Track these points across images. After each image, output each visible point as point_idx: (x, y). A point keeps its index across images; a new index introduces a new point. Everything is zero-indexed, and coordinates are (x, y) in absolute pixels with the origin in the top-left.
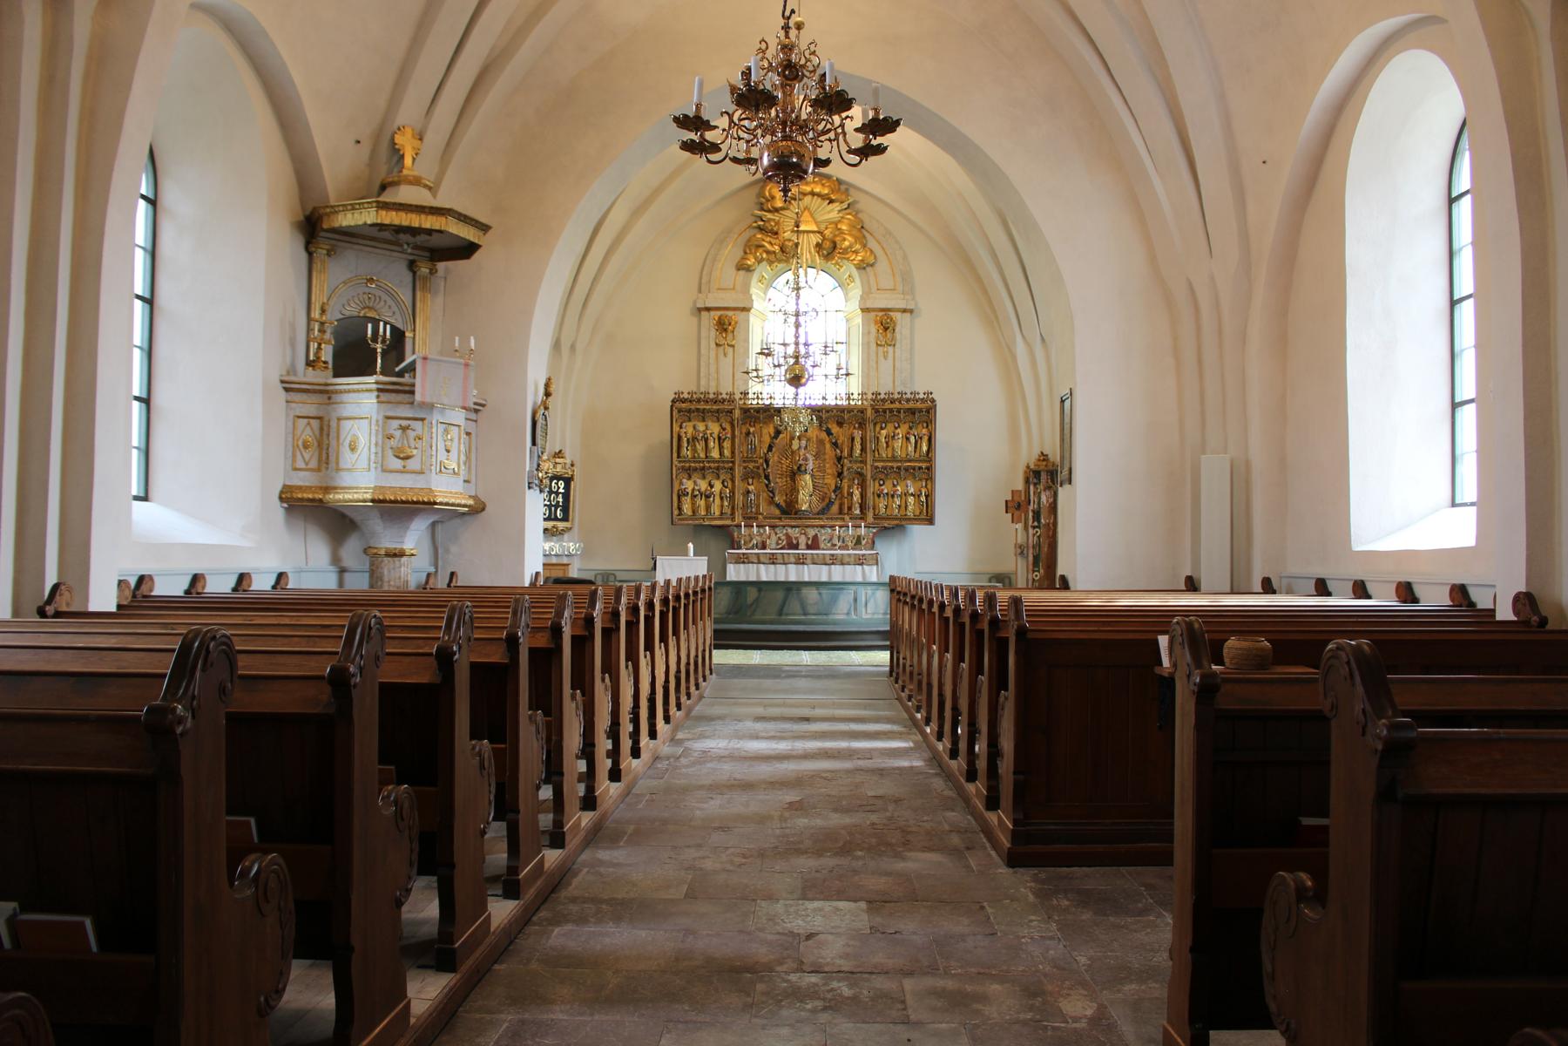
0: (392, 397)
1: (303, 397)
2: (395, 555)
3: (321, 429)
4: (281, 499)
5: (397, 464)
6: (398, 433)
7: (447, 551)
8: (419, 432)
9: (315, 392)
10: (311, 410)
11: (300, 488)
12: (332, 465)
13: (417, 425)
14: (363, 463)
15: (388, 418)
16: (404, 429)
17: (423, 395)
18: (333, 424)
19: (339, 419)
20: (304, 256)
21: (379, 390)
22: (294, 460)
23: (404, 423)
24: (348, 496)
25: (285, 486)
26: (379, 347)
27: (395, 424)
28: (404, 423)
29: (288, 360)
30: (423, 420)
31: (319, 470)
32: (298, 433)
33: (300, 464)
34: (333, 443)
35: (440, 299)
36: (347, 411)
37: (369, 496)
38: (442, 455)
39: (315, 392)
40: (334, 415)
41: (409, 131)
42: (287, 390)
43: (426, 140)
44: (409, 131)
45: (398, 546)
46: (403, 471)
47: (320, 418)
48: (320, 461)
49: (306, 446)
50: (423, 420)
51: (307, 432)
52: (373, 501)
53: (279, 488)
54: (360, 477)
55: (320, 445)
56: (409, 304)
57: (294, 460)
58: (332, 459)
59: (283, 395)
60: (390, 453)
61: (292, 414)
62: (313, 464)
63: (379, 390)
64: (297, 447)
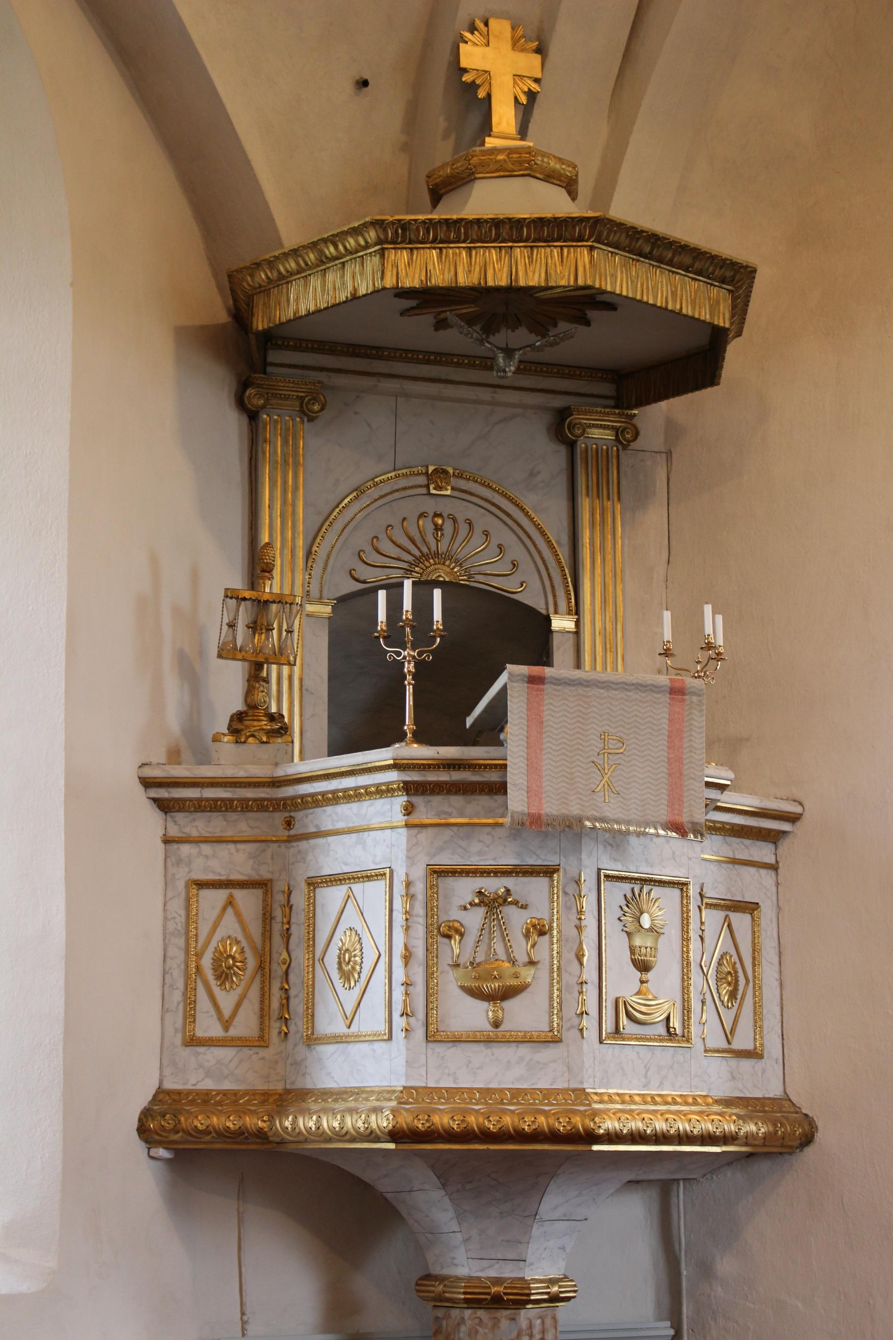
0: (455, 809)
1: (216, 824)
2: (497, 1302)
3: (267, 917)
4: (142, 1130)
5: (474, 1015)
6: (474, 919)
7: (706, 1270)
8: (540, 910)
9: (245, 806)
10: (234, 861)
11: (204, 1100)
12: (298, 1025)
13: (534, 890)
14: (372, 1018)
15: (438, 873)
16: (492, 904)
17: (533, 792)
18: (299, 900)
19: (314, 883)
20: (233, 423)
21: (409, 788)
22: (190, 1016)
23: (494, 885)
24: (331, 1123)
25: (161, 1095)
26: (408, 658)
27: (464, 889)
28: (494, 885)
29: (173, 721)
30: (549, 872)
31: (262, 1041)
32: (204, 930)
33: (208, 1025)
34: (300, 955)
35: (654, 517)
36: (335, 855)
37: (383, 1122)
38: (621, 981)
39: (245, 806)
40: (301, 875)
41: (500, 28)
42: (164, 806)
43: (554, 50)
44: (500, 28)
45: (508, 1272)
46: (495, 1036)
47: (263, 885)
48: (263, 1014)
49: (223, 976)
50: (549, 872)
51: (227, 926)
52: (395, 1135)
53: (143, 1099)
54: (368, 1063)
55: (263, 967)
56: (558, 530)
57: (190, 1016)
58: (297, 1005)
59: (153, 823)
60: (450, 984)
61: (182, 876)
62: (246, 1024)
63: (409, 788)
64: (198, 971)
